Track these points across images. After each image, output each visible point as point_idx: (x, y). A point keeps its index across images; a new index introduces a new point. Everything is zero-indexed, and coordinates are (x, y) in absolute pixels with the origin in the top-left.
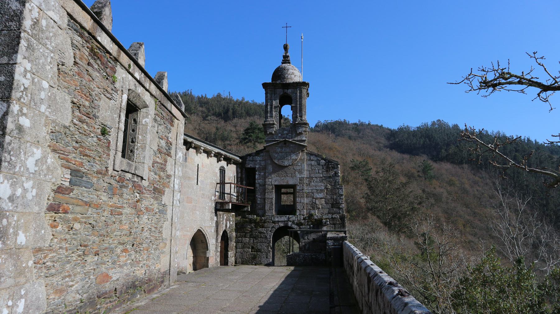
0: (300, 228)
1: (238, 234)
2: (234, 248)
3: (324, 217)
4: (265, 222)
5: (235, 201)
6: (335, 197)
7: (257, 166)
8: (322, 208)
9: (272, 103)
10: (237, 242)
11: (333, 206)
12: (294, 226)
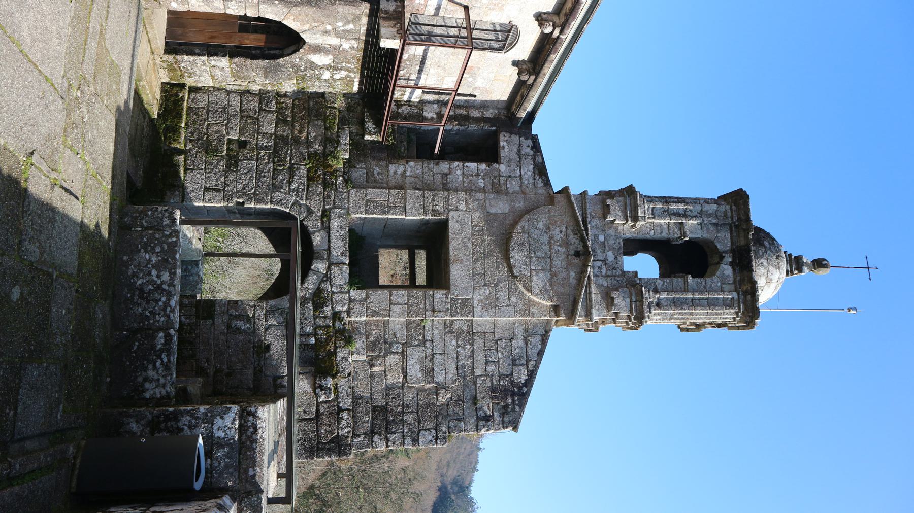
0: (304, 301)
1: (289, 102)
2: (244, 85)
3: (342, 382)
4: (325, 185)
5: (397, 95)
6: (409, 418)
7: (503, 168)
8: (372, 376)
9: (692, 217)
10: (262, 96)
11: (380, 412)
12: (312, 282)
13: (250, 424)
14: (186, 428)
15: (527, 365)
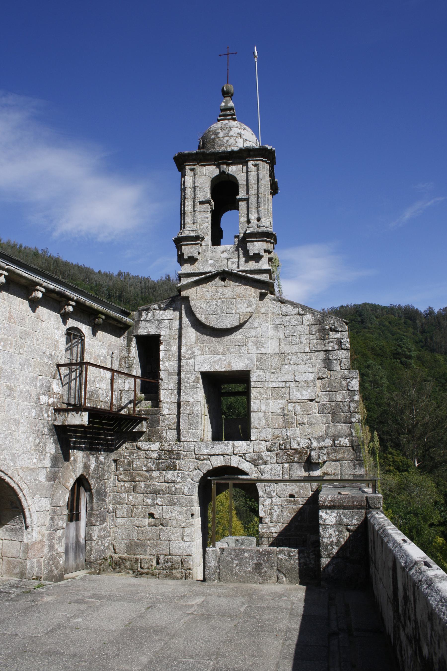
4: (179, 459)
7: (162, 333)
12: (246, 466)
13: (329, 505)
14: (331, 540)
15: (302, 315)
